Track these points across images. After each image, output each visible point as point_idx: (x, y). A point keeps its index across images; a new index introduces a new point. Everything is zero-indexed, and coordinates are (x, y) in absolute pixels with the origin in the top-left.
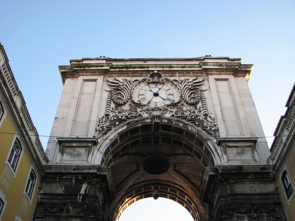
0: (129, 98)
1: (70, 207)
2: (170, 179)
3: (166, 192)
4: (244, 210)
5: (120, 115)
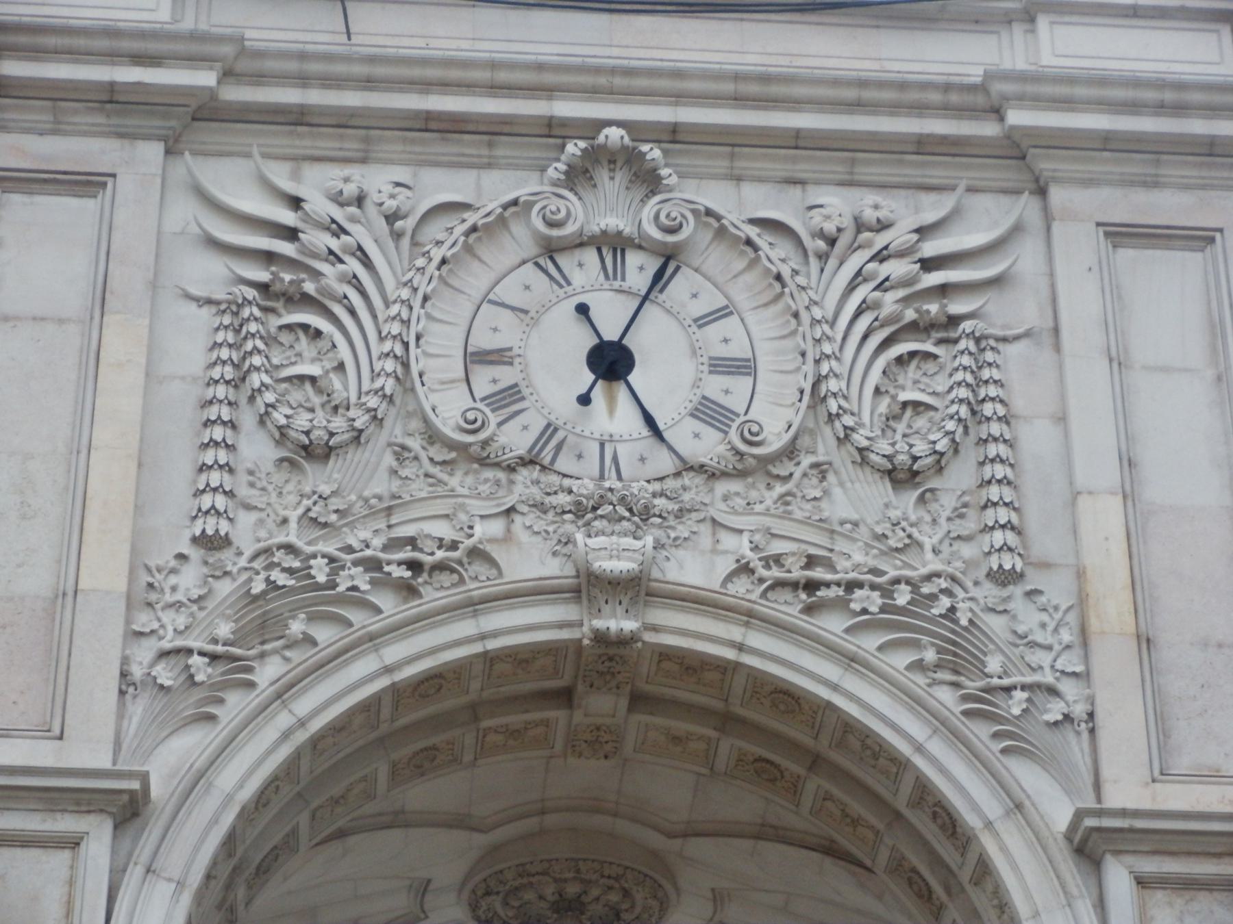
0: (390, 385)
5: (321, 547)
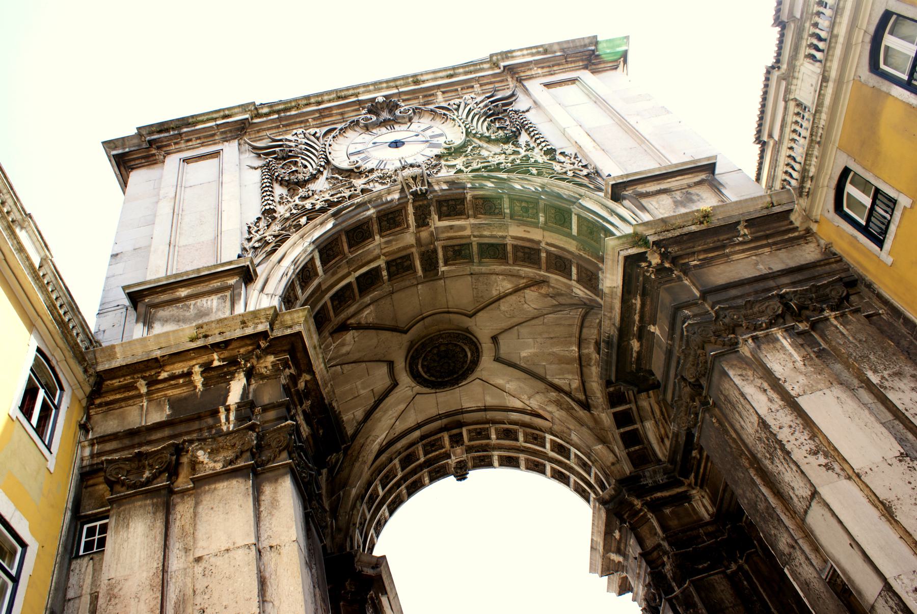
2: (490, 401)
3: (485, 448)
4: (763, 319)
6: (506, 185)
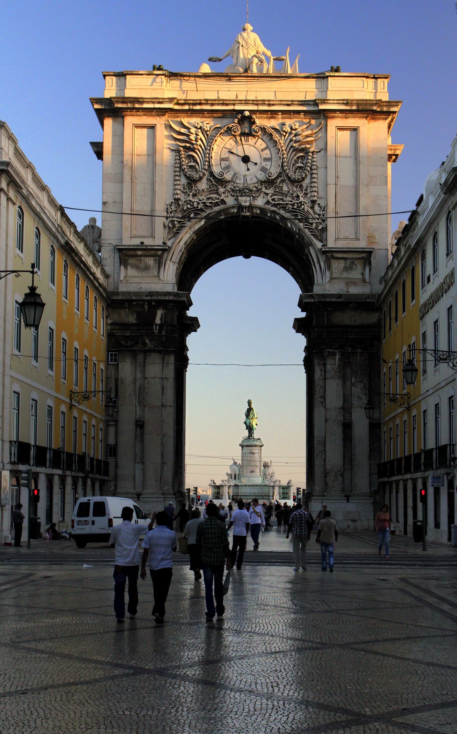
0: (207, 168)
1: (147, 340)
5: (196, 200)
6: (285, 221)
